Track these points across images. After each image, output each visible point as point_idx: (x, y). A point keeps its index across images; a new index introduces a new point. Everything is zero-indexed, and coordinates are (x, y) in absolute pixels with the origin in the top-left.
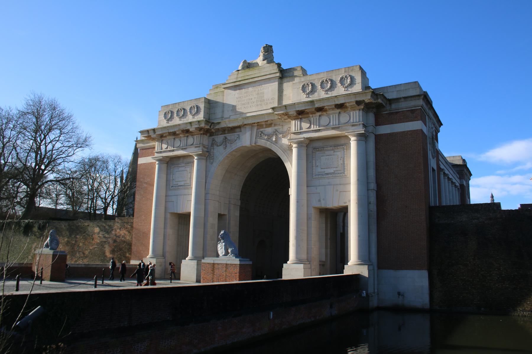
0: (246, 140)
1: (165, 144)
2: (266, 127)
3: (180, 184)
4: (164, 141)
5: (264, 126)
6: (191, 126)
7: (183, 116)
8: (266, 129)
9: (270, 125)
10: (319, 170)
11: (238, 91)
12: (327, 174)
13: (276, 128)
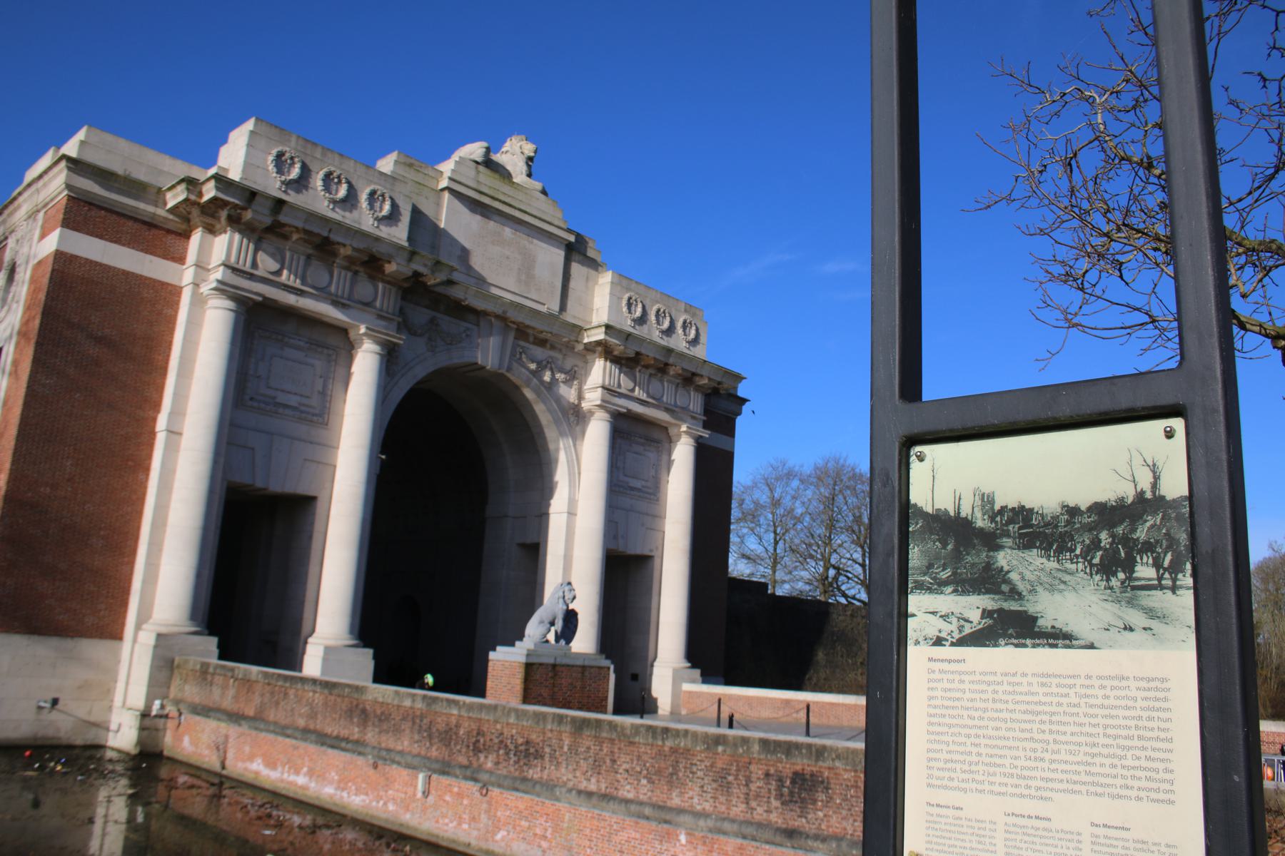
0: (488, 353)
1: (272, 256)
2: (534, 343)
3: (282, 398)
4: (264, 246)
5: (531, 339)
6: (410, 260)
7: (344, 201)
8: (531, 346)
9: (542, 343)
10: (622, 477)
11: (478, 217)
12: (632, 489)
13: (552, 353)
